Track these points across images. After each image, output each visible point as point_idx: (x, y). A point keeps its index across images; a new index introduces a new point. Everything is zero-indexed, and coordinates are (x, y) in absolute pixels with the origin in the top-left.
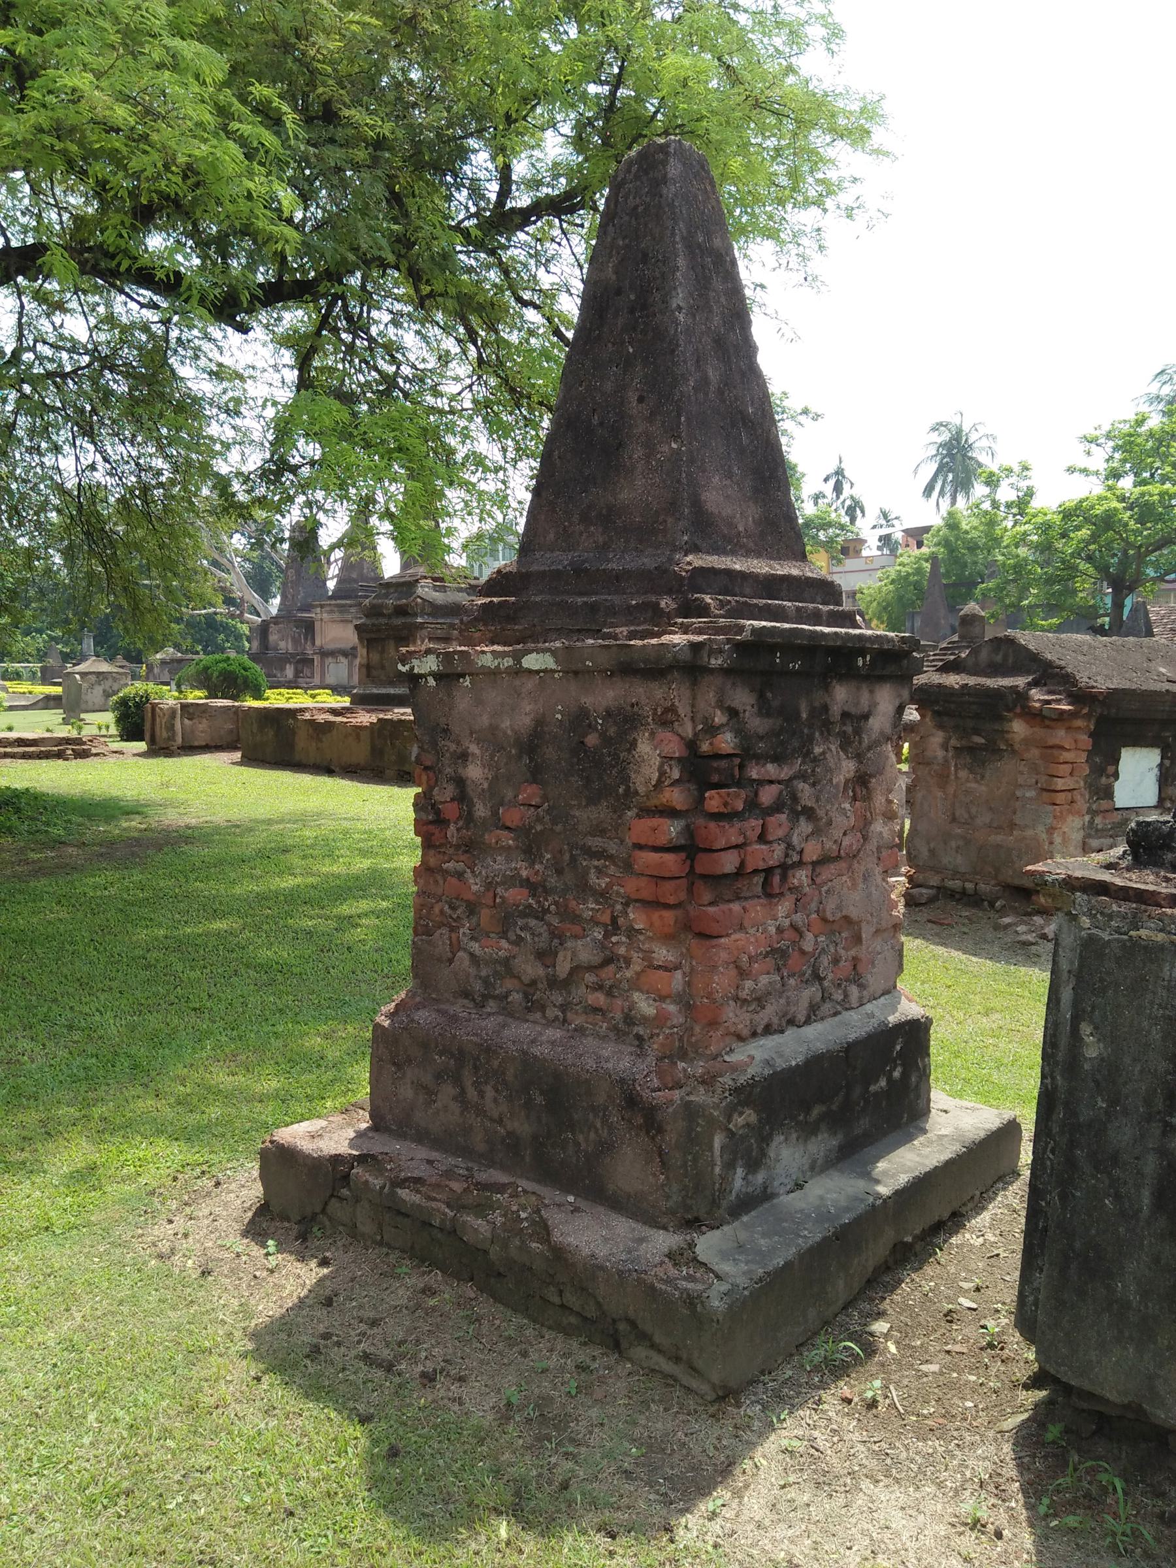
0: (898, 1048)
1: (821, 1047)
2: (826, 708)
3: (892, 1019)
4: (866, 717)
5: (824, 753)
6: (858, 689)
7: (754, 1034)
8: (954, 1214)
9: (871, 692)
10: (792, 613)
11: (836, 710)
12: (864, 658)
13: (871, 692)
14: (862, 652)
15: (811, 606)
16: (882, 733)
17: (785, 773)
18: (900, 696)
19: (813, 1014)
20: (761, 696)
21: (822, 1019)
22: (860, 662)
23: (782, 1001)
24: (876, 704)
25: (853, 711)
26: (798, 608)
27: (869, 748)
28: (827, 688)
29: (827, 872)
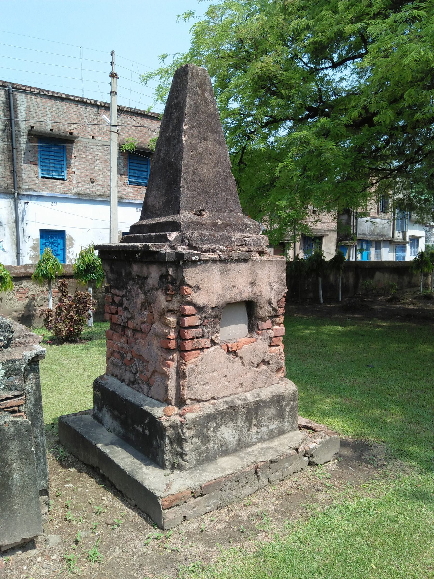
0: (147, 421)
1: (119, 392)
2: (130, 273)
3: (146, 407)
4: (146, 278)
5: (130, 289)
6: (142, 266)
7: (116, 376)
8: (121, 492)
9: (148, 268)
10: (142, 238)
11: (134, 274)
12: (138, 254)
13: (148, 268)
14: (137, 252)
15: (148, 234)
16: (153, 285)
17: (121, 294)
18: (161, 271)
19: (131, 383)
20: (111, 267)
21: (133, 388)
22: (137, 256)
23: (121, 371)
24: (150, 274)
25: (140, 275)
26: (144, 236)
27: (148, 291)
28: (130, 265)
29: (138, 335)
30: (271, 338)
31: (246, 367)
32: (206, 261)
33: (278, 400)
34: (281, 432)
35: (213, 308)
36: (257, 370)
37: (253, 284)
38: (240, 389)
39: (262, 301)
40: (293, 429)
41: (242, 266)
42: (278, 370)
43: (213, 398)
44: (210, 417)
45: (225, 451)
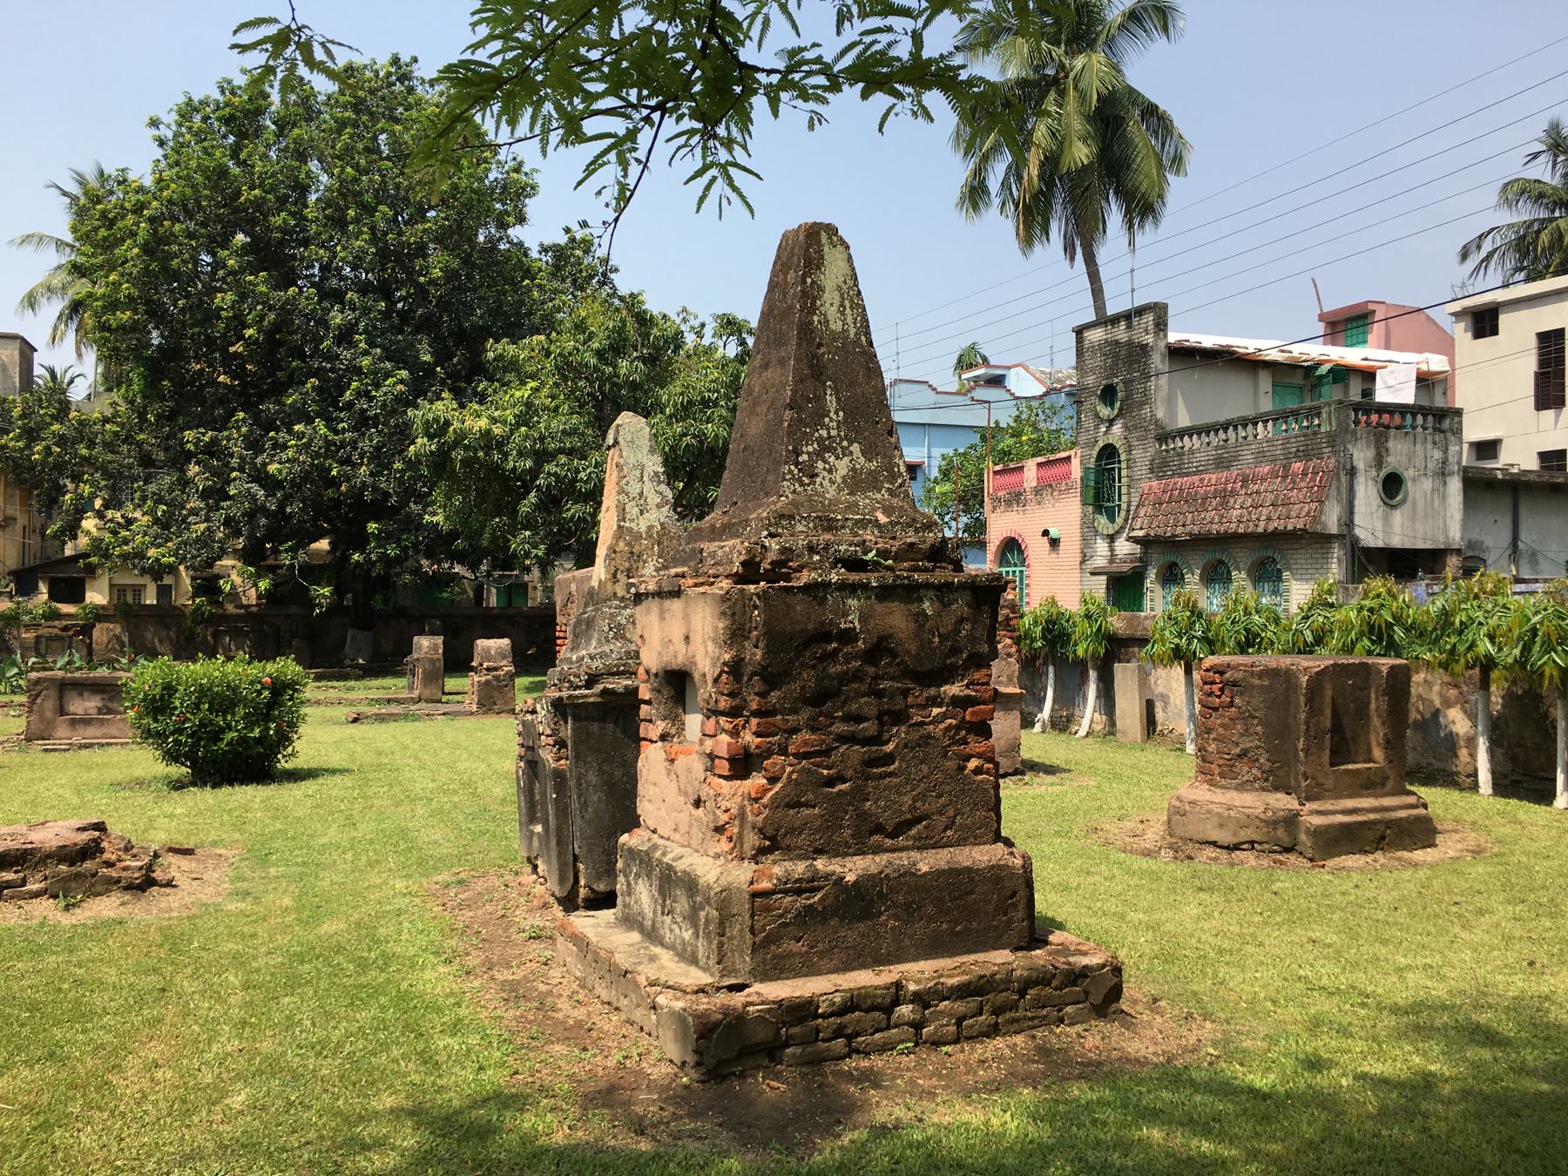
30: (712, 757)
31: (682, 799)
32: (647, 595)
33: (690, 884)
34: (693, 961)
35: (656, 675)
36: (694, 811)
37: (687, 638)
38: (677, 837)
39: (696, 676)
40: (705, 969)
41: (676, 605)
42: (719, 830)
43: (654, 832)
44: (632, 853)
45: (641, 928)
